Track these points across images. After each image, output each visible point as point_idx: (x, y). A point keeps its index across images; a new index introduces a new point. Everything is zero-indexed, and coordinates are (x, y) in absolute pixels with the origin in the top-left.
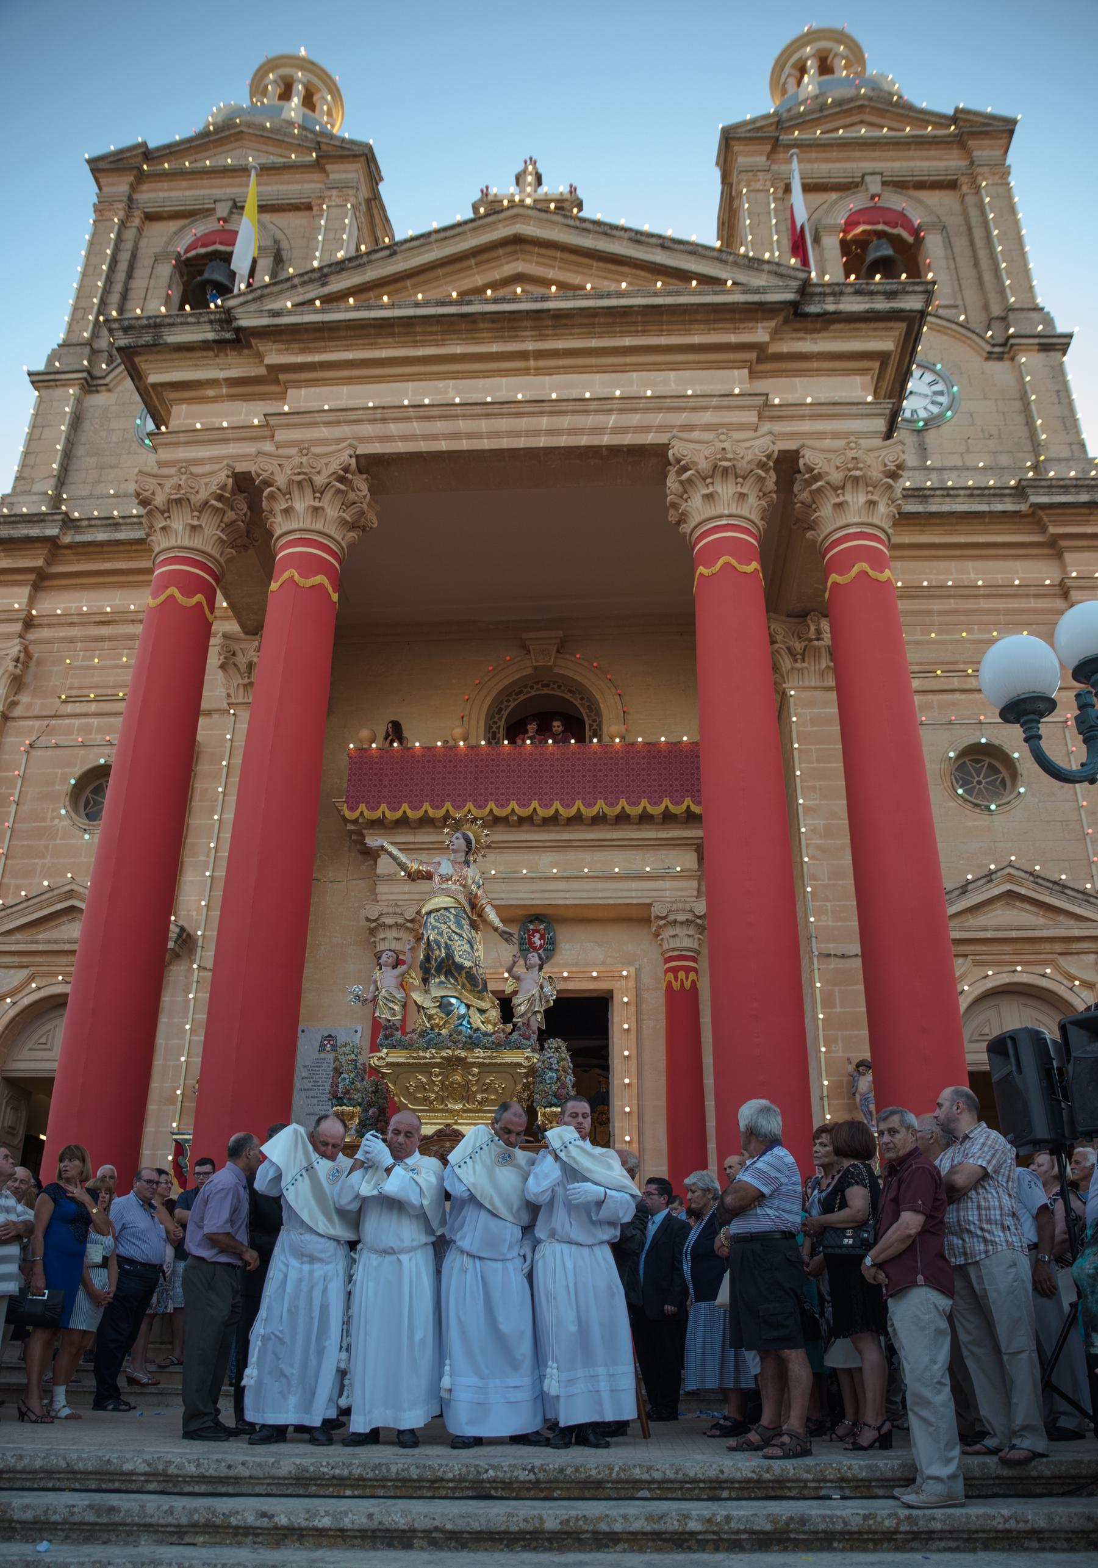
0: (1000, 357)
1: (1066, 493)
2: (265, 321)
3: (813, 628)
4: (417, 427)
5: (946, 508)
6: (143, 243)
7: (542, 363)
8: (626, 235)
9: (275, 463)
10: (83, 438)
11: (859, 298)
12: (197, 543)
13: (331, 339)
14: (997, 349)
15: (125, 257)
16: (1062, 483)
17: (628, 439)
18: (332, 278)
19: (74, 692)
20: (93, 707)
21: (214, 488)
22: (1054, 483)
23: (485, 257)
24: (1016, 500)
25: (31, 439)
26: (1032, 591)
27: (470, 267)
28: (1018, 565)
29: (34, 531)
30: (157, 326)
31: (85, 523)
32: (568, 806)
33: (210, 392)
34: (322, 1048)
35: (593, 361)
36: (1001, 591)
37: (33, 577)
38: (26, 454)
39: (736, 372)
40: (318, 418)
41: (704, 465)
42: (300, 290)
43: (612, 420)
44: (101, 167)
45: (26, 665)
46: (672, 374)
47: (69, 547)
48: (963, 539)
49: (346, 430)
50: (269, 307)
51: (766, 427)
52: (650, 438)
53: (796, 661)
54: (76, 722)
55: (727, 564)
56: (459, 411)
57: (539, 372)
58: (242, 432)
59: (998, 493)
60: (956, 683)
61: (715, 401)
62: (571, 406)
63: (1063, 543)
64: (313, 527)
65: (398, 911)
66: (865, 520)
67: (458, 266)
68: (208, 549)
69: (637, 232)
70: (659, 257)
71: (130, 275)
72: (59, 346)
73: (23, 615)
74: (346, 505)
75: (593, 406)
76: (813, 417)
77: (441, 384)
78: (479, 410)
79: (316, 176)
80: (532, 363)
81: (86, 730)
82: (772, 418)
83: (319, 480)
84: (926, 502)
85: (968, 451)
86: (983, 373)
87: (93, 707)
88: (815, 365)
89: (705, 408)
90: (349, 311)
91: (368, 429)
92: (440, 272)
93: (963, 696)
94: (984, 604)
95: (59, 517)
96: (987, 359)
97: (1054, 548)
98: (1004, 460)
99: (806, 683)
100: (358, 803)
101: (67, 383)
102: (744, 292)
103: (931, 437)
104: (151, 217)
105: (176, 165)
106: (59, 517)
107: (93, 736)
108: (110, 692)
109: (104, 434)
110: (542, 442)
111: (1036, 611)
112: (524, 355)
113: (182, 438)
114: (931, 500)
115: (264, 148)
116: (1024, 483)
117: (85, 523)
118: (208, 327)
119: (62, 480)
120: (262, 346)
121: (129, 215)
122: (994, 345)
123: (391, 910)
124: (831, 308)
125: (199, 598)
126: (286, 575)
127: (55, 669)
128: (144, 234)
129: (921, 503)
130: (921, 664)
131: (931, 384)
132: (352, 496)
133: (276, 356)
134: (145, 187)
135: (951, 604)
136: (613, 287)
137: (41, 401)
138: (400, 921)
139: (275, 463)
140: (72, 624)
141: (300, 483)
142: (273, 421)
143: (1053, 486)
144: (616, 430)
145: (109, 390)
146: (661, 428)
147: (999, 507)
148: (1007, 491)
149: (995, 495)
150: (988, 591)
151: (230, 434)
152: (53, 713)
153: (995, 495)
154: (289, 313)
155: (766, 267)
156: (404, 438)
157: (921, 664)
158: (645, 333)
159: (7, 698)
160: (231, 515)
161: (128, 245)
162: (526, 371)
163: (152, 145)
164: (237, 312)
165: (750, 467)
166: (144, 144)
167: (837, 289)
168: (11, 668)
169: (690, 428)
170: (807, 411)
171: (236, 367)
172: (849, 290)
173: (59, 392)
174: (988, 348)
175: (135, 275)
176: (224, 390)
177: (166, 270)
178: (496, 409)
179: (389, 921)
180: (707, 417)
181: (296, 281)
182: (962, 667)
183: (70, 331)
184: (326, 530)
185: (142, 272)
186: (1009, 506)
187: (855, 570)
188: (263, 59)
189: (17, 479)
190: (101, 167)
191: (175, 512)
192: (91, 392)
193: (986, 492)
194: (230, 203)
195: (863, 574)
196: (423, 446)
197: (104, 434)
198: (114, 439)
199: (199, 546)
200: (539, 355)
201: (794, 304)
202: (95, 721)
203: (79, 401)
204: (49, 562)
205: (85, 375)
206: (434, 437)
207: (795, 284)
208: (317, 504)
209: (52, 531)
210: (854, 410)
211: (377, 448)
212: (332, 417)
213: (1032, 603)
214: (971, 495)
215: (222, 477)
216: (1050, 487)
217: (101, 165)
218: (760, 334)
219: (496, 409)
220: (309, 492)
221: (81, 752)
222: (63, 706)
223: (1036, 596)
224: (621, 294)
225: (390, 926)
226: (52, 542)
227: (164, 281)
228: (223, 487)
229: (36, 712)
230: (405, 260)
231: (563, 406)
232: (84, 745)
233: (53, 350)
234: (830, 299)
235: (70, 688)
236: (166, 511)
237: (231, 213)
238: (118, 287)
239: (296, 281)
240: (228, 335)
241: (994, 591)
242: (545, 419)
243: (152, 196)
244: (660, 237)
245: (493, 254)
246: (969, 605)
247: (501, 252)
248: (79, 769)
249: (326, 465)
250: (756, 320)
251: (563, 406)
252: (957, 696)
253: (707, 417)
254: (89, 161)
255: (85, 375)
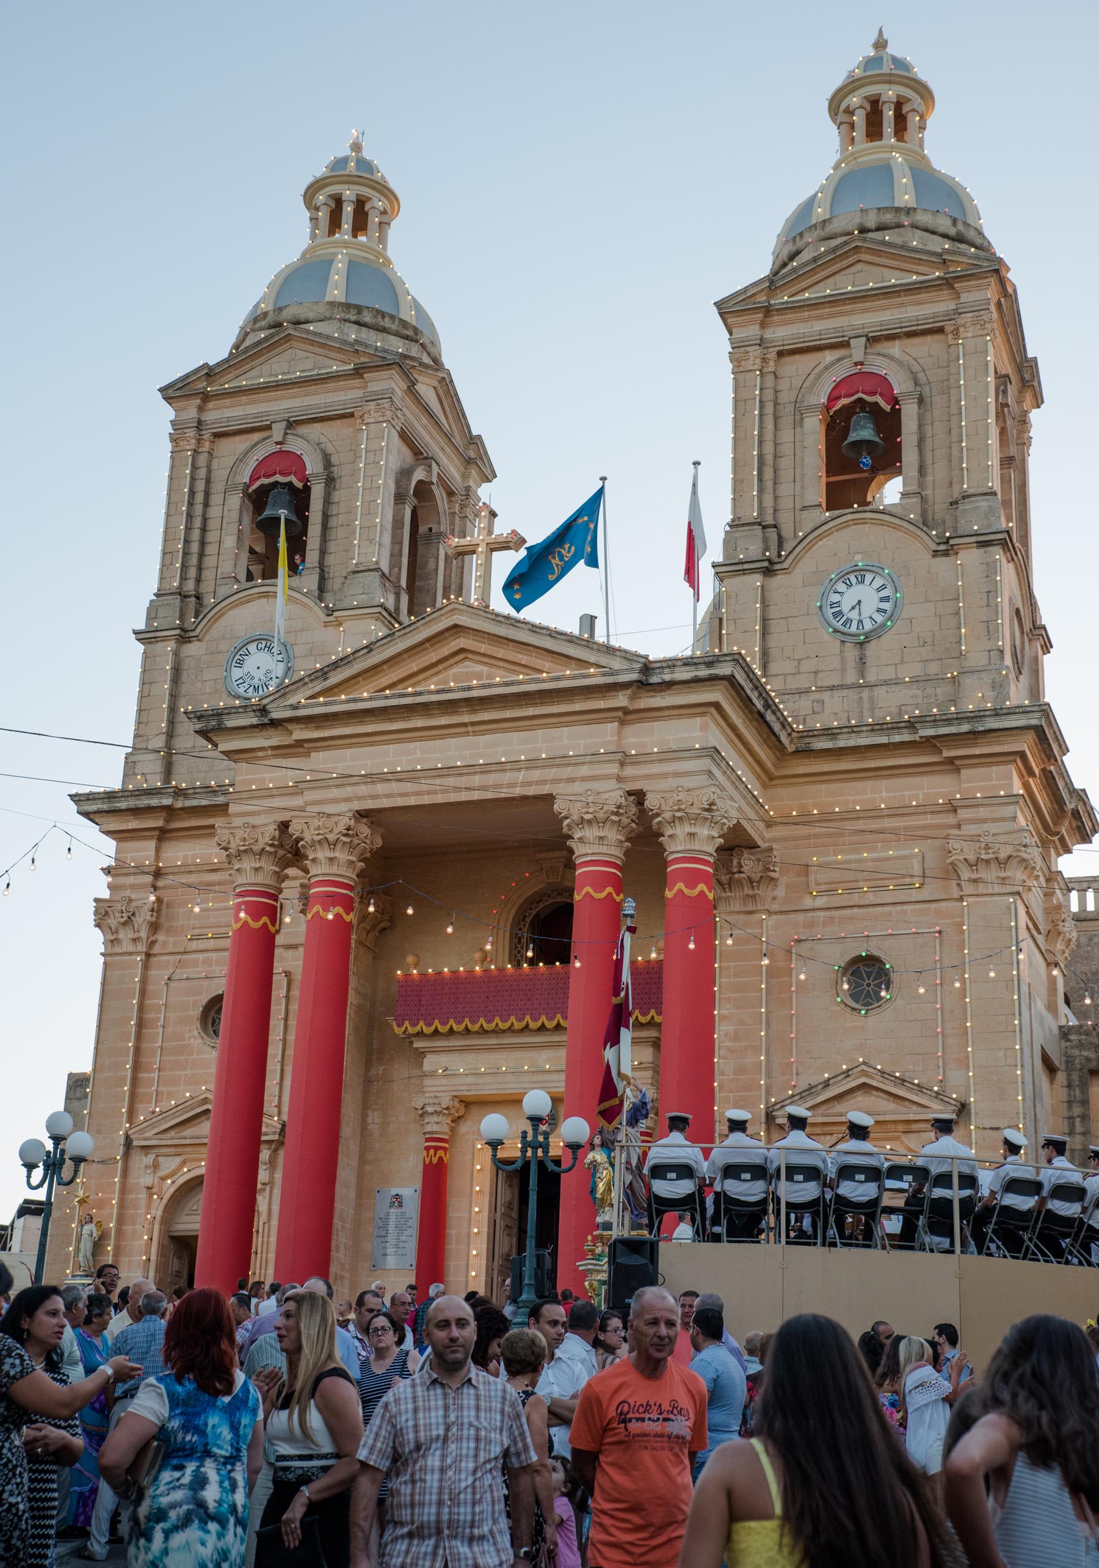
0: (946, 553)
1: (952, 725)
2: (288, 714)
3: (735, 862)
4: (395, 787)
5: (852, 743)
6: (215, 464)
7: (477, 728)
8: (526, 627)
9: (302, 822)
10: (184, 689)
11: (688, 668)
12: (260, 879)
13: (334, 720)
14: (942, 547)
15: (200, 486)
16: (944, 717)
17: (532, 791)
18: (331, 674)
19: (197, 932)
20: (211, 944)
21: (267, 840)
22: (938, 717)
23: (436, 640)
24: (911, 731)
25: (142, 696)
26: (928, 809)
27: (427, 648)
28: (926, 780)
29: (154, 802)
30: (218, 715)
31: (191, 791)
32: (551, 1019)
33: (260, 754)
34: (392, 1205)
35: (511, 724)
36: (901, 811)
37: (157, 833)
38: (140, 711)
39: (609, 725)
40: (330, 783)
41: (575, 817)
42: (310, 685)
43: (521, 776)
44: (173, 392)
45: (159, 911)
46: (565, 729)
47: (181, 809)
48: (873, 764)
49: (348, 791)
50: (288, 703)
51: (629, 771)
52: (545, 790)
53: (724, 889)
54: (201, 956)
55: (587, 892)
56: (421, 774)
57: (475, 733)
58: (284, 791)
59: (895, 727)
60: (856, 899)
61: (588, 759)
62: (494, 768)
63: (958, 762)
64: (331, 872)
65: (436, 1101)
66: (689, 847)
67: (417, 650)
68: (268, 882)
69: (533, 625)
70: (549, 644)
71: (206, 505)
72: (155, 595)
73: (153, 869)
74: (351, 847)
75: (509, 766)
76: (660, 761)
77: (411, 746)
78: (433, 773)
79: (356, 382)
80: (470, 729)
81: (208, 962)
82: (632, 763)
83: (332, 837)
84: (836, 739)
85: (902, 662)
86: (929, 572)
87: (211, 944)
88: (666, 713)
89: (583, 763)
90: (341, 703)
91: (363, 790)
92: (406, 656)
93: (861, 911)
94: (888, 823)
95: (171, 790)
96: (934, 556)
97: (952, 765)
98: (933, 668)
99: (733, 908)
100: (404, 1020)
101: (165, 639)
102: (604, 675)
103: (871, 649)
104: (218, 435)
105: (234, 384)
106: (171, 790)
107: (213, 968)
108: (222, 930)
109: (199, 685)
110: (476, 796)
111: (931, 827)
112: (465, 725)
113: (244, 795)
114: (839, 736)
115: (311, 348)
116: (912, 720)
117: (191, 791)
118: (252, 714)
119: (170, 734)
120: (290, 727)
121: (199, 441)
122: (938, 544)
123: (431, 1101)
124: (667, 677)
125: (265, 919)
126: (315, 910)
127: (181, 910)
128: (215, 455)
129: (831, 740)
130: (828, 883)
131: (879, 590)
132: (356, 841)
133: (300, 733)
134: (210, 405)
135: (861, 825)
136: (514, 678)
137: (146, 655)
138: (438, 1109)
139: (302, 822)
140: (190, 872)
141: (319, 842)
142: (301, 785)
143: (935, 721)
144: (524, 784)
145: (199, 640)
146: (555, 781)
147: (897, 738)
148: (903, 725)
149: (892, 728)
150: (890, 812)
151: (275, 792)
152: (182, 950)
153: (892, 728)
154: (305, 707)
155: (618, 653)
156: (387, 796)
157: (828, 883)
158: (542, 704)
159: (148, 938)
160: (281, 852)
161: (202, 473)
162: (467, 733)
163: (211, 363)
164: (268, 707)
165: (606, 816)
166: (206, 365)
167: (670, 663)
168: (148, 918)
169: (571, 780)
170: (655, 757)
171: (275, 739)
172: (679, 663)
173: (160, 645)
174: (934, 547)
175: (211, 503)
176: (270, 752)
177: (235, 501)
178: (444, 772)
179: (430, 1109)
180: (584, 771)
181: (306, 680)
182: (861, 884)
183: (162, 578)
184: (340, 872)
185: (216, 499)
186: (906, 737)
187: (676, 888)
188: (310, 180)
189: (135, 736)
190: (173, 392)
191: (244, 856)
192: (185, 642)
193: (885, 726)
194: (284, 424)
195: (680, 891)
196: (400, 802)
197: (199, 685)
198: (208, 690)
199: (262, 882)
200: (473, 724)
201: (639, 681)
202: (214, 955)
203: (176, 654)
204: (167, 821)
205: (178, 632)
206: (406, 795)
207: (638, 666)
208: (332, 855)
209: (167, 801)
210: (687, 754)
211: (370, 805)
212: (339, 781)
213: (930, 820)
214: (873, 730)
215: (273, 827)
216: (935, 721)
217: (171, 393)
218: (621, 700)
219: (444, 772)
220: (326, 846)
221: (206, 983)
222: (190, 943)
223: (932, 813)
224: (520, 683)
225: (432, 1114)
226: (169, 809)
227: (235, 515)
228: (273, 839)
229: (171, 950)
230: (379, 653)
231: (489, 768)
232: (207, 977)
233: (151, 601)
234: (667, 671)
235: (194, 928)
236: (240, 854)
237: (286, 434)
238: (197, 523)
239: (306, 680)
240: (266, 721)
241: (897, 812)
242: (477, 777)
243: (219, 414)
244: (547, 629)
245: (442, 637)
246: (875, 825)
247: (447, 634)
248: (205, 999)
249: (336, 823)
250: (617, 691)
251: (489, 768)
252: (856, 910)
253: (584, 771)
254: (161, 390)
255: (178, 632)
